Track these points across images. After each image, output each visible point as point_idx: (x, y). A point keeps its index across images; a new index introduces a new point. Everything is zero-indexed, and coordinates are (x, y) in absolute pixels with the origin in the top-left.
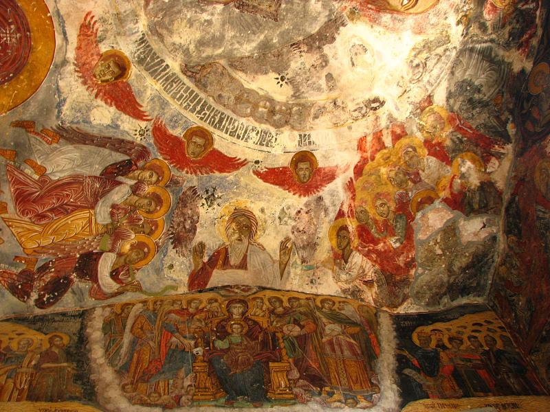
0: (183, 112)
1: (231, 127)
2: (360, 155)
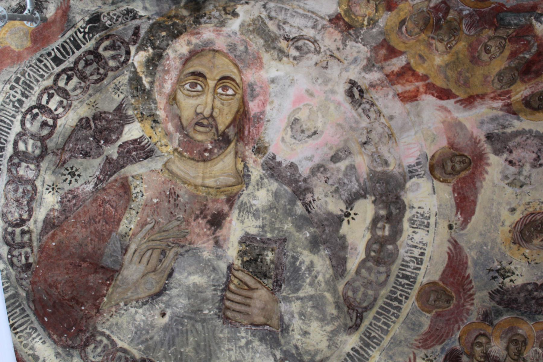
0: (401, 319)
1: (411, 264)
2: (424, 96)
